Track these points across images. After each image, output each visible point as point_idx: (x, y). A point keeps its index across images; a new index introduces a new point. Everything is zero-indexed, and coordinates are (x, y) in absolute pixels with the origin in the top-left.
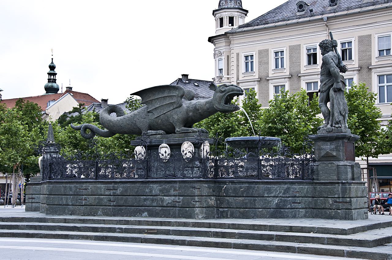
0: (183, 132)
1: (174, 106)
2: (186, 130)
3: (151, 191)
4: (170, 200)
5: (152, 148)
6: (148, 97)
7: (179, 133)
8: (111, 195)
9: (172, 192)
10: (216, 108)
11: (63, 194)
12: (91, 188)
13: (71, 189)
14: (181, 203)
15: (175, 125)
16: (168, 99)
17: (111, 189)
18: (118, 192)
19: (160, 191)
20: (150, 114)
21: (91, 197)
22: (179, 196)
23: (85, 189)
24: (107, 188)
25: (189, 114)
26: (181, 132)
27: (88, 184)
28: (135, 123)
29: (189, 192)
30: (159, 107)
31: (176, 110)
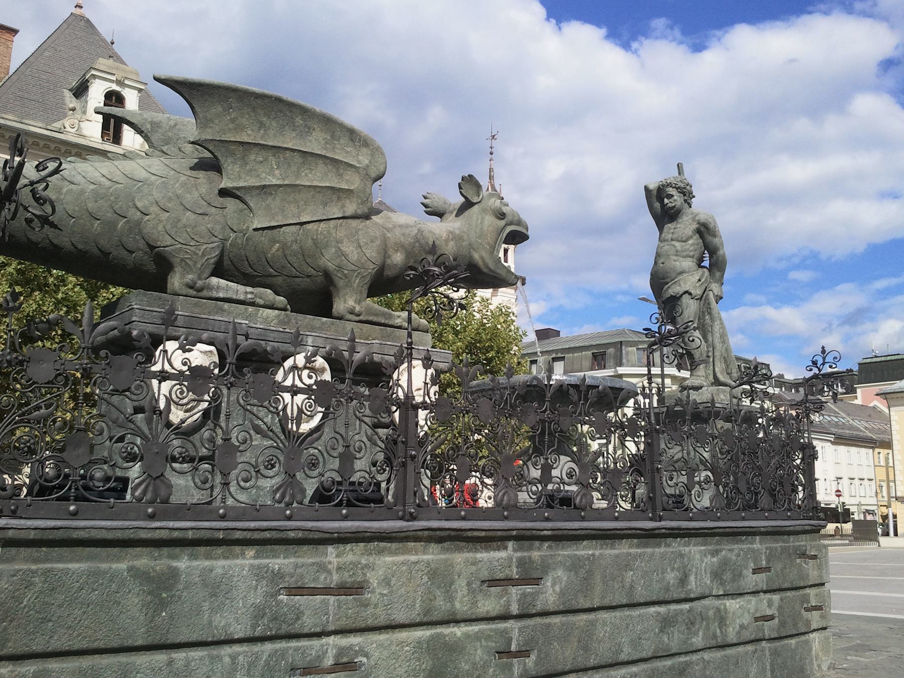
0: (370, 318)
1: (343, 206)
2: (384, 315)
3: (683, 581)
4: (746, 615)
5: (251, 363)
6: (231, 126)
7: (357, 318)
8: (504, 617)
9: (751, 580)
10: (480, 263)
11: (140, 642)
12: (386, 582)
13: (217, 589)
14: (776, 621)
15: (341, 283)
16: (321, 166)
17: (509, 581)
18: (549, 594)
19: (716, 575)
20: (231, 204)
21: (383, 637)
22: (765, 592)
23: (344, 589)
24: (485, 574)
25: (389, 257)
26: (361, 318)
27: (352, 554)
28: (138, 223)
29: (793, 577)
30: (280, 186)
31: (354, 223)
